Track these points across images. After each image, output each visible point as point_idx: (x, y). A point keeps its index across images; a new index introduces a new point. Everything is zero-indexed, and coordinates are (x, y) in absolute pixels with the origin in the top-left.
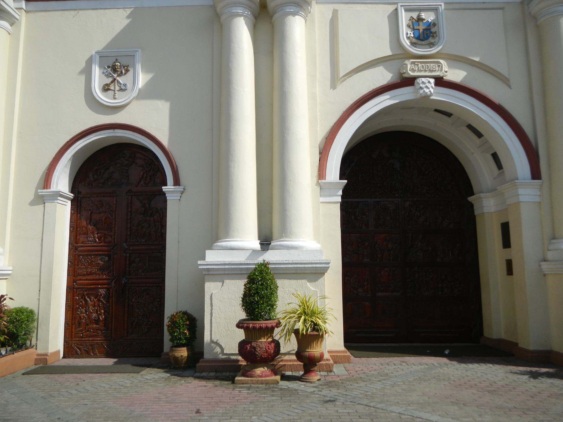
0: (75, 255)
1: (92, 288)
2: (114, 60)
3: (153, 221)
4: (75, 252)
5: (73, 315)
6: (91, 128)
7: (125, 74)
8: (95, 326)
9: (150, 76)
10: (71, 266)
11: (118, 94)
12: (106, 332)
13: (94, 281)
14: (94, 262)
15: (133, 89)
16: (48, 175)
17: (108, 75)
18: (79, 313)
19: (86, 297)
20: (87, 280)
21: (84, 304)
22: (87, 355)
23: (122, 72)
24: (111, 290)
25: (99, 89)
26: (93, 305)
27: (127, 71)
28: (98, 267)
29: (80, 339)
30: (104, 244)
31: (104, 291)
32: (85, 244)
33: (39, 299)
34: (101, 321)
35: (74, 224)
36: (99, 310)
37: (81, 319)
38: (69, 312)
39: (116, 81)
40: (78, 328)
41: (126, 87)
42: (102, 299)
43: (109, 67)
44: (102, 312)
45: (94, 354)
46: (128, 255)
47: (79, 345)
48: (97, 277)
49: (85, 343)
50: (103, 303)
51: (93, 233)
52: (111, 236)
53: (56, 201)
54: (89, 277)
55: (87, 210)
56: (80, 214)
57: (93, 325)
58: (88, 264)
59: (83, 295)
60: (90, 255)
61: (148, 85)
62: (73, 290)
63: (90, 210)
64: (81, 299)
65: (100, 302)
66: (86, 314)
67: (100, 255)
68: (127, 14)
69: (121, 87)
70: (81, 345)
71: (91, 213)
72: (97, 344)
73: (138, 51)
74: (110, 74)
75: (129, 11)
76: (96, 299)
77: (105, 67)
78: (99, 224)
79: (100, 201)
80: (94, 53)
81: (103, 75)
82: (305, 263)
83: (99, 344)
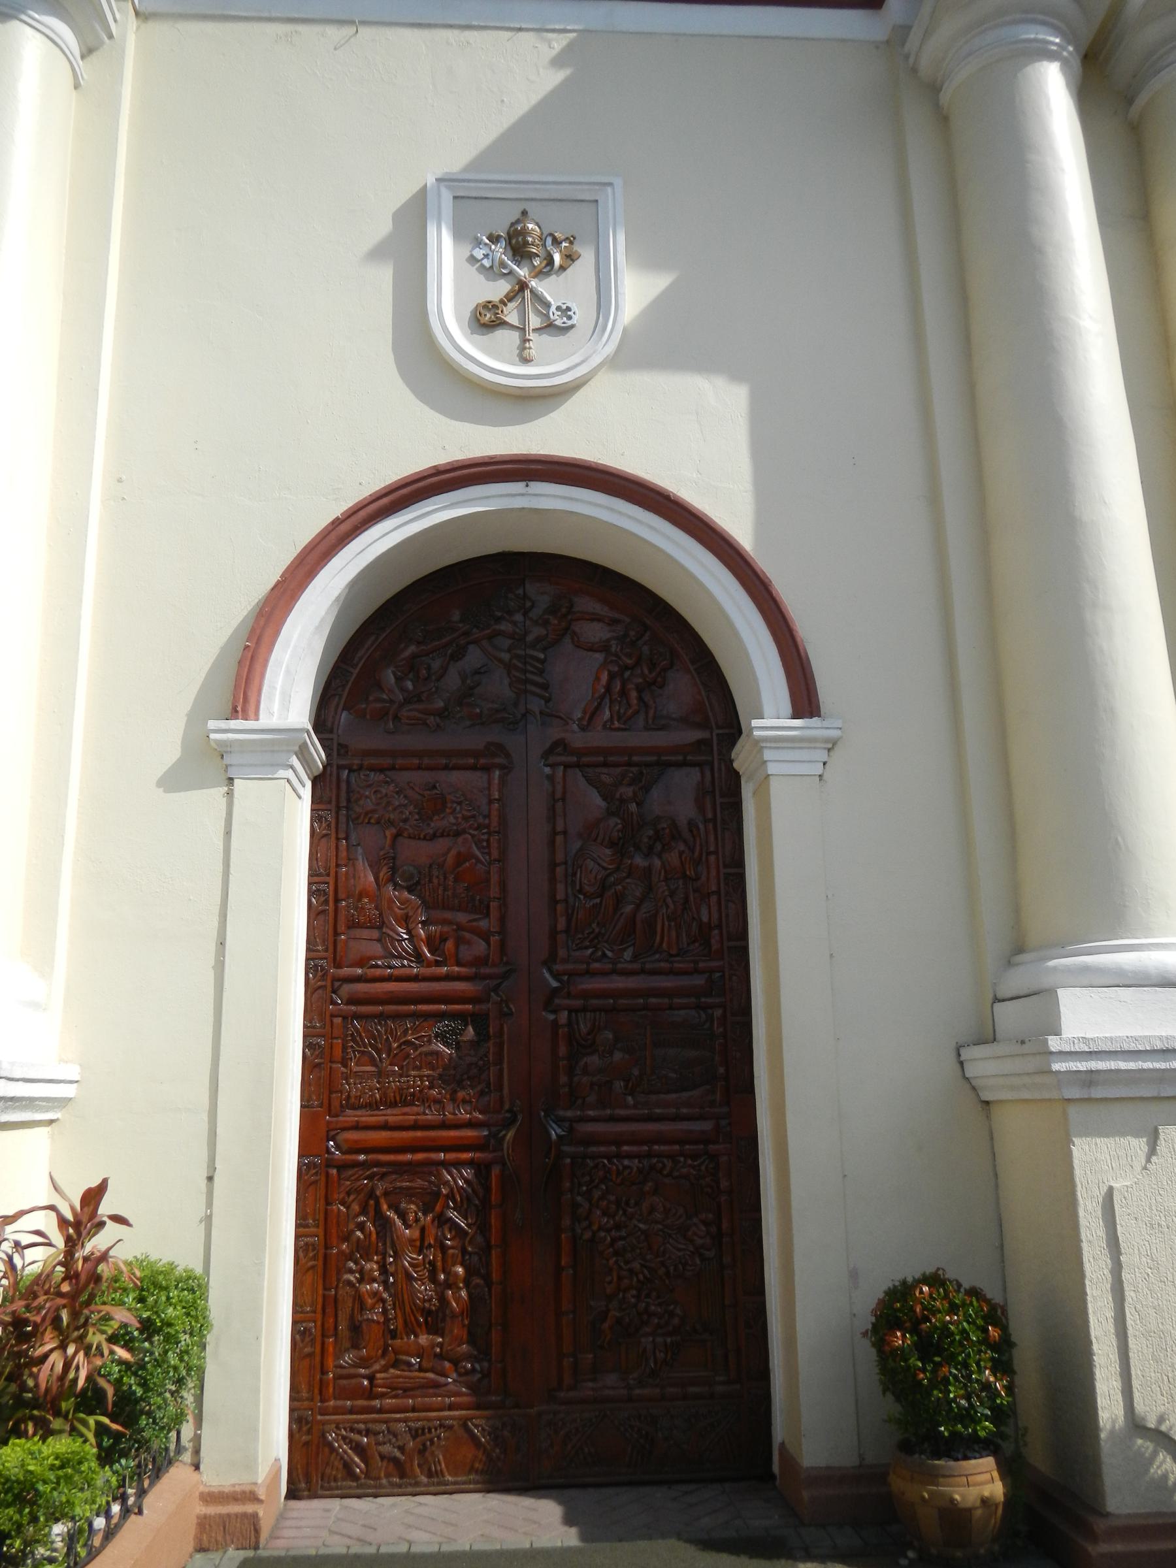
0: (333, 1016)
1: (409, 1163)
2: (516, 215)
3: (663, 873)
4: (333, 1003)
5: (325, 1289)
6: (437, 471)
7: (563, 268)
8: (424, 1339)
9: (658, 283)
10: (317, 1065)
11: (537, 342)
12: (477, 1366)
13: (419, 1134)
14: (415, 1049)
15: (599, 326)
16: (252, 657)
17: (491, 267)
18: (352, 1278)
19: (385, 1207)
20: (385, 1127)
21: (374, 1236)
22: (396, 1480)
23: (550, 261)
24: (496, 1171)
25: (459, 319)
26: (418, 1243)
27: (570, 258)
28: (433, 1069)
29: (361, 1403)
30: (456, 969)
31: (462, 1177)
32: (373, 966)
33: (208, 1220)
34: (454, 1316)
35: (327, 879)
36: (439, 1264)
37: (362, 1307)
38: (309, 1277)
39: (527, 293)
40: (347, 1350)
41: (570, 318)
42: (453, 1214)
43: (494, 239)
44: (456, 1274)
45: (430, 1475)
46: (563, 1016)
47: (359, 1432)
48: (431, 1116)
49: (386, 1422)
50: (459, 1232)
51: (405, 921)
52: (485, 936)
53: (282, 773)
54: (392, 1116)
55: (378, 822)
56: (346, 839)
57: (416, 1336)
58: (388, 1055)
59: (371, 1194)
60: (397, 1016)
61: (656, 310)
62: (327, 1175)
63: (391, 823)
64: (357, 1216)
65: (446, 1228)
66: (385, 1283)
67: (441, 1016)
68: (554, 52)
69: (547, 316)
70: (368, 1433)
71: (396, 837)
72: (441, 1426)
73: (610, 184)
74: (503, 264)
75: (559, 43)
76: (425, 1214)
77: (476, 239)
78: (430, 881)
79: (434, 787)
80: (431, 180)
81: (473, 270)
82: (1139, 1052)
83: (451, 1427)
